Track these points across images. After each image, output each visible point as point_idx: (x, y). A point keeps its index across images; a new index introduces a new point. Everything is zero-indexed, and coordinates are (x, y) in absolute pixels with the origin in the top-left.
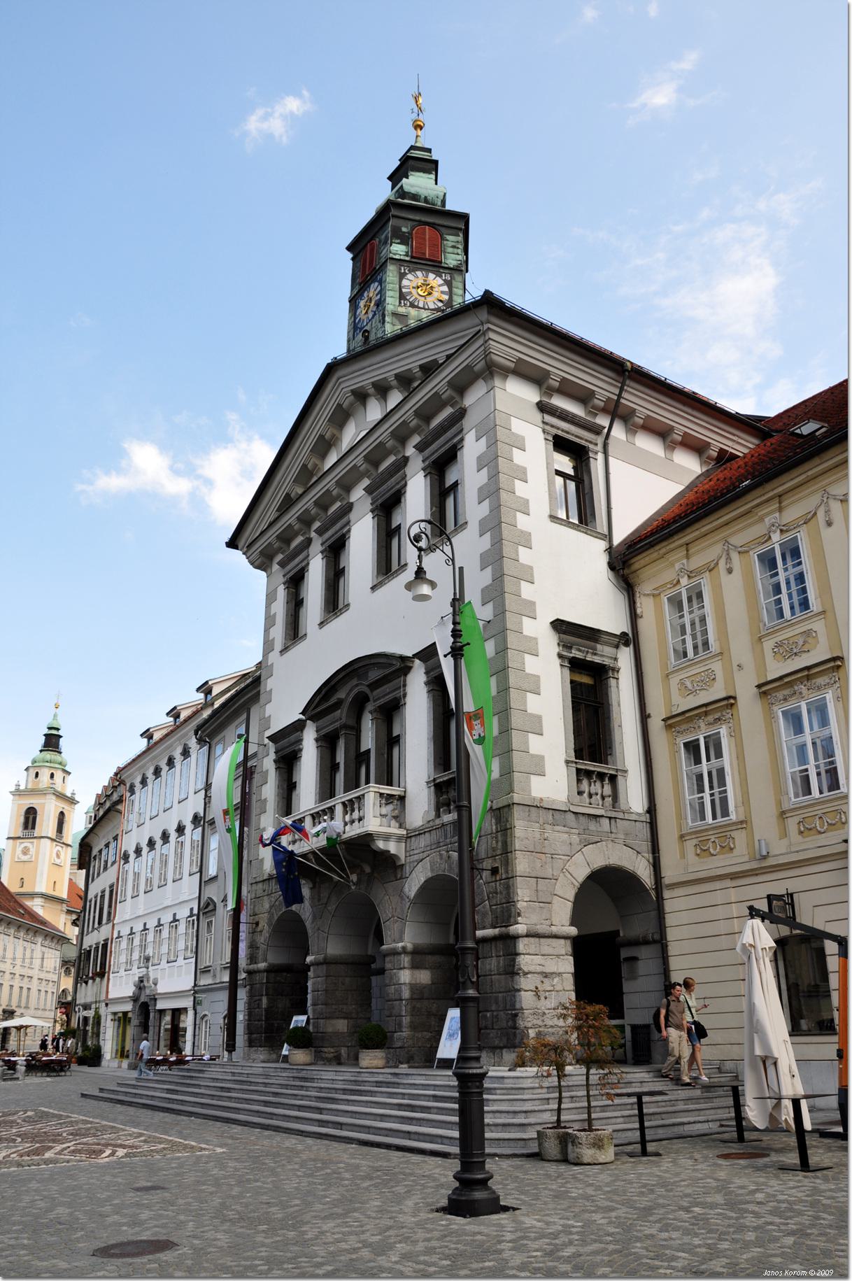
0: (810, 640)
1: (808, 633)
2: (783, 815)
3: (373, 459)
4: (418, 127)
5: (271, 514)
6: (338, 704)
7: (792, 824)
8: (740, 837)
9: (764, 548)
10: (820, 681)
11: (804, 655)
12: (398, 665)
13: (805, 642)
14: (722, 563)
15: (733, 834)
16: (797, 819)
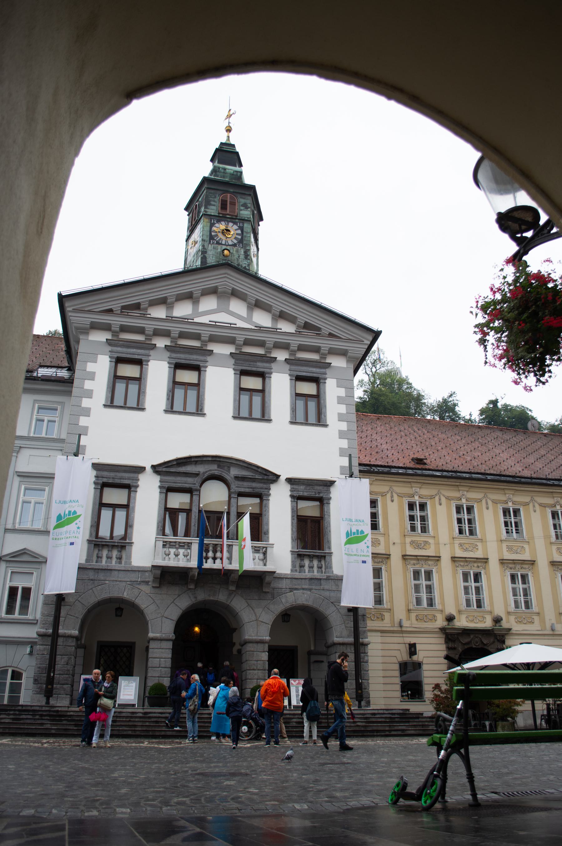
0: (427, 545)
1: (426, 542)
2: (409, 611)
3: (248, 342)
4: (229, 130)
5: (116, 306)
6: (197, 475)
7: (413, 616)
8: (387, 615)
9: (411, 500)
10: (430, 562)
11: (424, 550)
12: (271, 477)
13: (425, 545)
14: (389, 496)
15: (384, 613)
16: (415, 614)
